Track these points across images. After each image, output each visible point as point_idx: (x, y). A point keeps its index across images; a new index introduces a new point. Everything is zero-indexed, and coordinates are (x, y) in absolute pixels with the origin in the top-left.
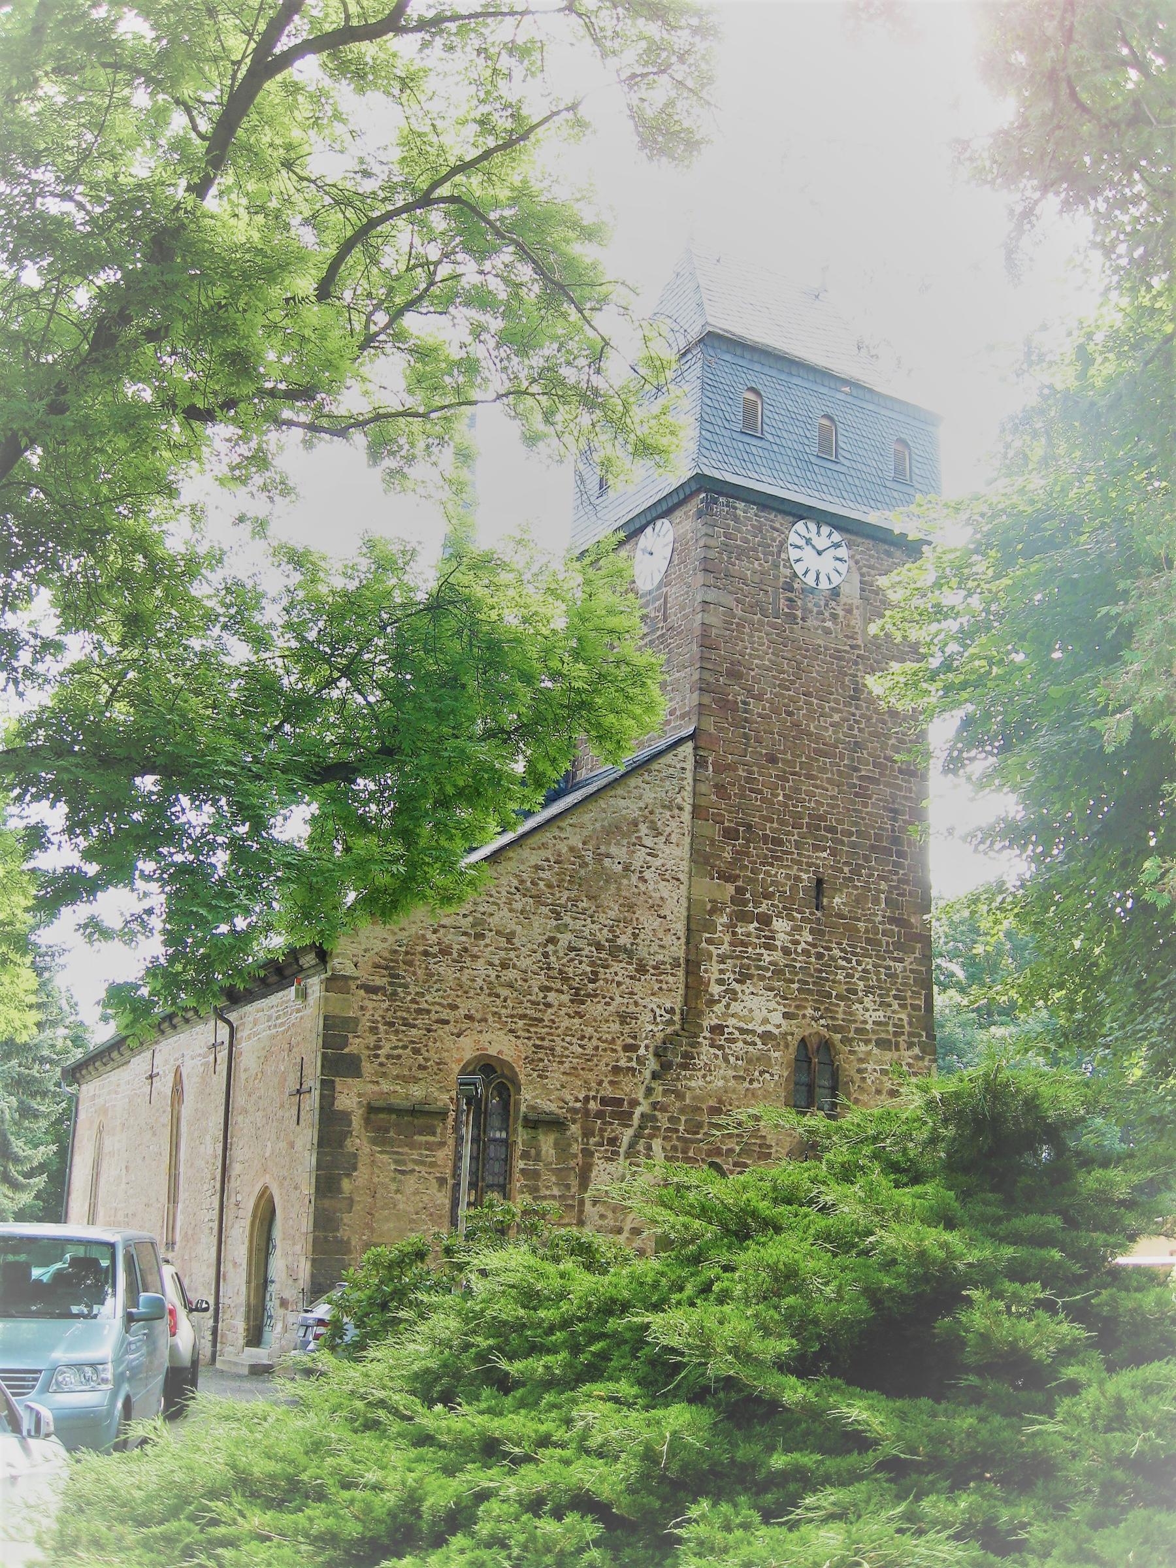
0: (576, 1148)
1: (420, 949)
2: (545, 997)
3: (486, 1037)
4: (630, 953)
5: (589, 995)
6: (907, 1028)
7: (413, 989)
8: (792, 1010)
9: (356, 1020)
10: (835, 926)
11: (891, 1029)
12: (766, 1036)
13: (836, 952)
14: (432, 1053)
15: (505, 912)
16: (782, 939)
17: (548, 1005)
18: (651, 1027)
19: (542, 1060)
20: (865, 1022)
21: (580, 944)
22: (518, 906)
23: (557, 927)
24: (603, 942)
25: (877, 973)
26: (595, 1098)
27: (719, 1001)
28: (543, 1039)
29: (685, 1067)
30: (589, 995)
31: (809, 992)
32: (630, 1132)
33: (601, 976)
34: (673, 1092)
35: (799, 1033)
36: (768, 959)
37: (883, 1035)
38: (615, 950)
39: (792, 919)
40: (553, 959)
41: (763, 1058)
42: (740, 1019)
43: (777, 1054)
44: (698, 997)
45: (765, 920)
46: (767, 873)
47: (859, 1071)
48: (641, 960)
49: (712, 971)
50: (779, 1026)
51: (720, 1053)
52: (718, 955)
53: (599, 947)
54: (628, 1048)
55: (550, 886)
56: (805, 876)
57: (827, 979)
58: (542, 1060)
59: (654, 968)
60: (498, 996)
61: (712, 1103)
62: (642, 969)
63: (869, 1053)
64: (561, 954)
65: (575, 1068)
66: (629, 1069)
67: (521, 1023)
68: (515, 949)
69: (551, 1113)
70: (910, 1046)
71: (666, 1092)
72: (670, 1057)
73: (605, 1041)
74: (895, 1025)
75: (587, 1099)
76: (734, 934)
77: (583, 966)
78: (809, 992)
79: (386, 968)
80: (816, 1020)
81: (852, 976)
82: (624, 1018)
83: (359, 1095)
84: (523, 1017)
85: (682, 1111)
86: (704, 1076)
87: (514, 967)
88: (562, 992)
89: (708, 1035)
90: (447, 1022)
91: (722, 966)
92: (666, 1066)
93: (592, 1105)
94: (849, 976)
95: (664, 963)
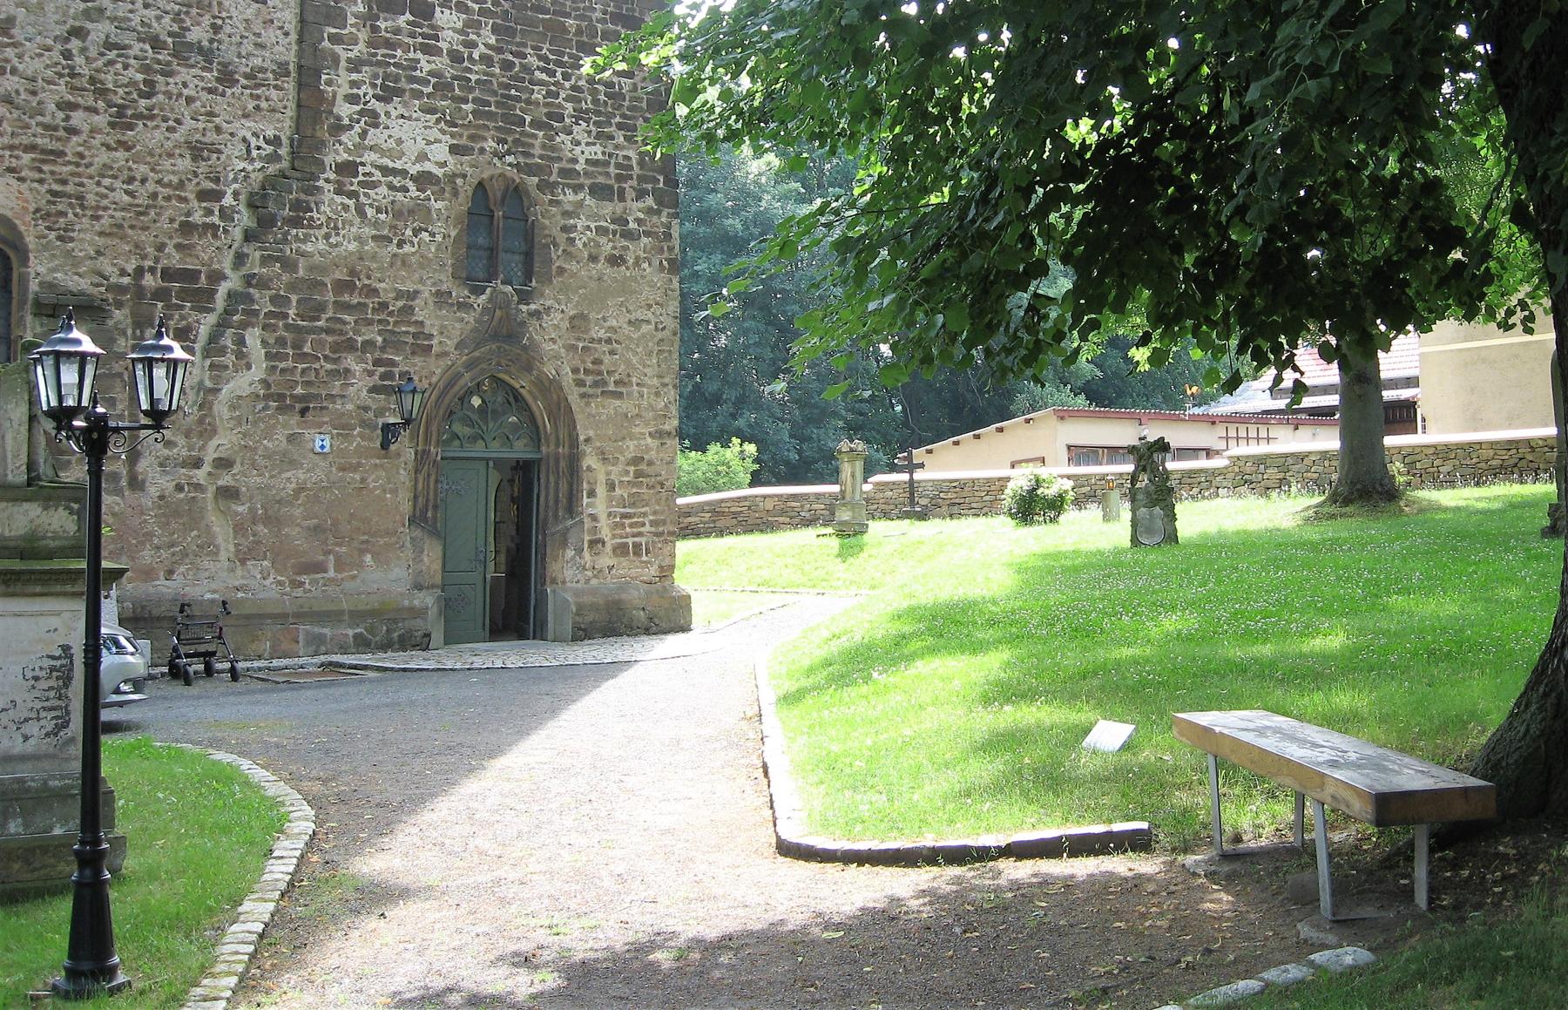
2: (68, 118)
4: (207, 55)
5: (140, 116)
6: (637, 170)
8: (463, 141)
10: (532, 23)
11: (612, 170)
12: (423, 179)
13: (533, 61)
16: (449, 39)
17: (73, 131)
18: (242, 165)
19: (63, 214)
20: (574, 161)
21: (127, 38)
23: (87, 14)
24: (164, 37)
25: (594, 92)
26: (152, 270)
27: (350, 127)
28: (64, 182)
29: (296, 222)
30: (140, 116)
31: (490, 116)
32: (211, 319)
33: (161, 87)
34: (277, 259)
35: (474, 175)
36: (427, 68)
37: (601, 180)
38: (183, 50)
40: (79, 60)
41: (419, 211)
42: (383, 153)
43: (439, 205)
44: (316, 119)
47: (565, 229)
48: (225, 65)
49: (338, 83)
50: (444, 164)
51: (351, 203)
52: (349, 60)
53: (156, 44)
54: (203, 195)
57: (518, 99)
58: (63, 214)
59: (246, 76)
61: (341, 274)
62: (227, 77)
63: (581, 204)
64: (93, 53)
65: (120, 226)
66: (206, 226)
67: (27, 158)
68: (14, 45)
69: (82, 293)
70: (640, 195)
71: (265, 261)
72: (272, 208)
73: (169, 185)
74: (618, 166)
75: (140, 272)
76: (375, 29)
77: (131, 72)
78: (490, 116)
81: (557, 95)
82: (197, 151)
84: (31, 148)
85: (292, 287)
86: (327, 237)
87: (14, 71)
88: (95, 111)
89: (332, 176)
91: (354, 76)
92: (266, 222)
93: (149, 281)
94: (549, 94)
95: (263, 70)
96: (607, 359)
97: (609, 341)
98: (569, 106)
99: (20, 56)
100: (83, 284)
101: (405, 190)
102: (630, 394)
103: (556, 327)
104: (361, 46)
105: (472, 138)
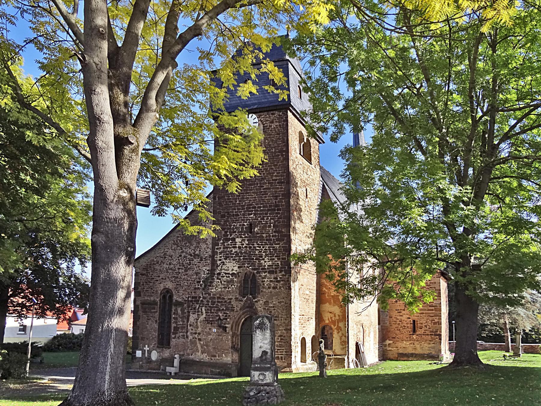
0: (186, 311)
3: (166, 283)
4: (198, 255)
15: (171, 250)
16: (238, 244)
17: (179, 273)
22: (173, 248)
36: (234, 251)
37: (271, 269)
38: (195, 256)
39: (241, 237)
45: (234, 239)
46: (234, 225)
47: (263, 281)
53: (191, 255)
55: (180, 241)
56: (245, 224)
62: (201, 260)
63: (266, 276)
75: (188, 297)
80: (248, 267)
82: (197, 274)
84: (174, 277)
94: (260, 252)
96: (273, 311)
97: (273, 307)
98: (264, 254)
100: (180, 300)
101: (229, 277)
102: (278, 320)
103: (261, 304)
104: (222, 249)
105: (242, 264)
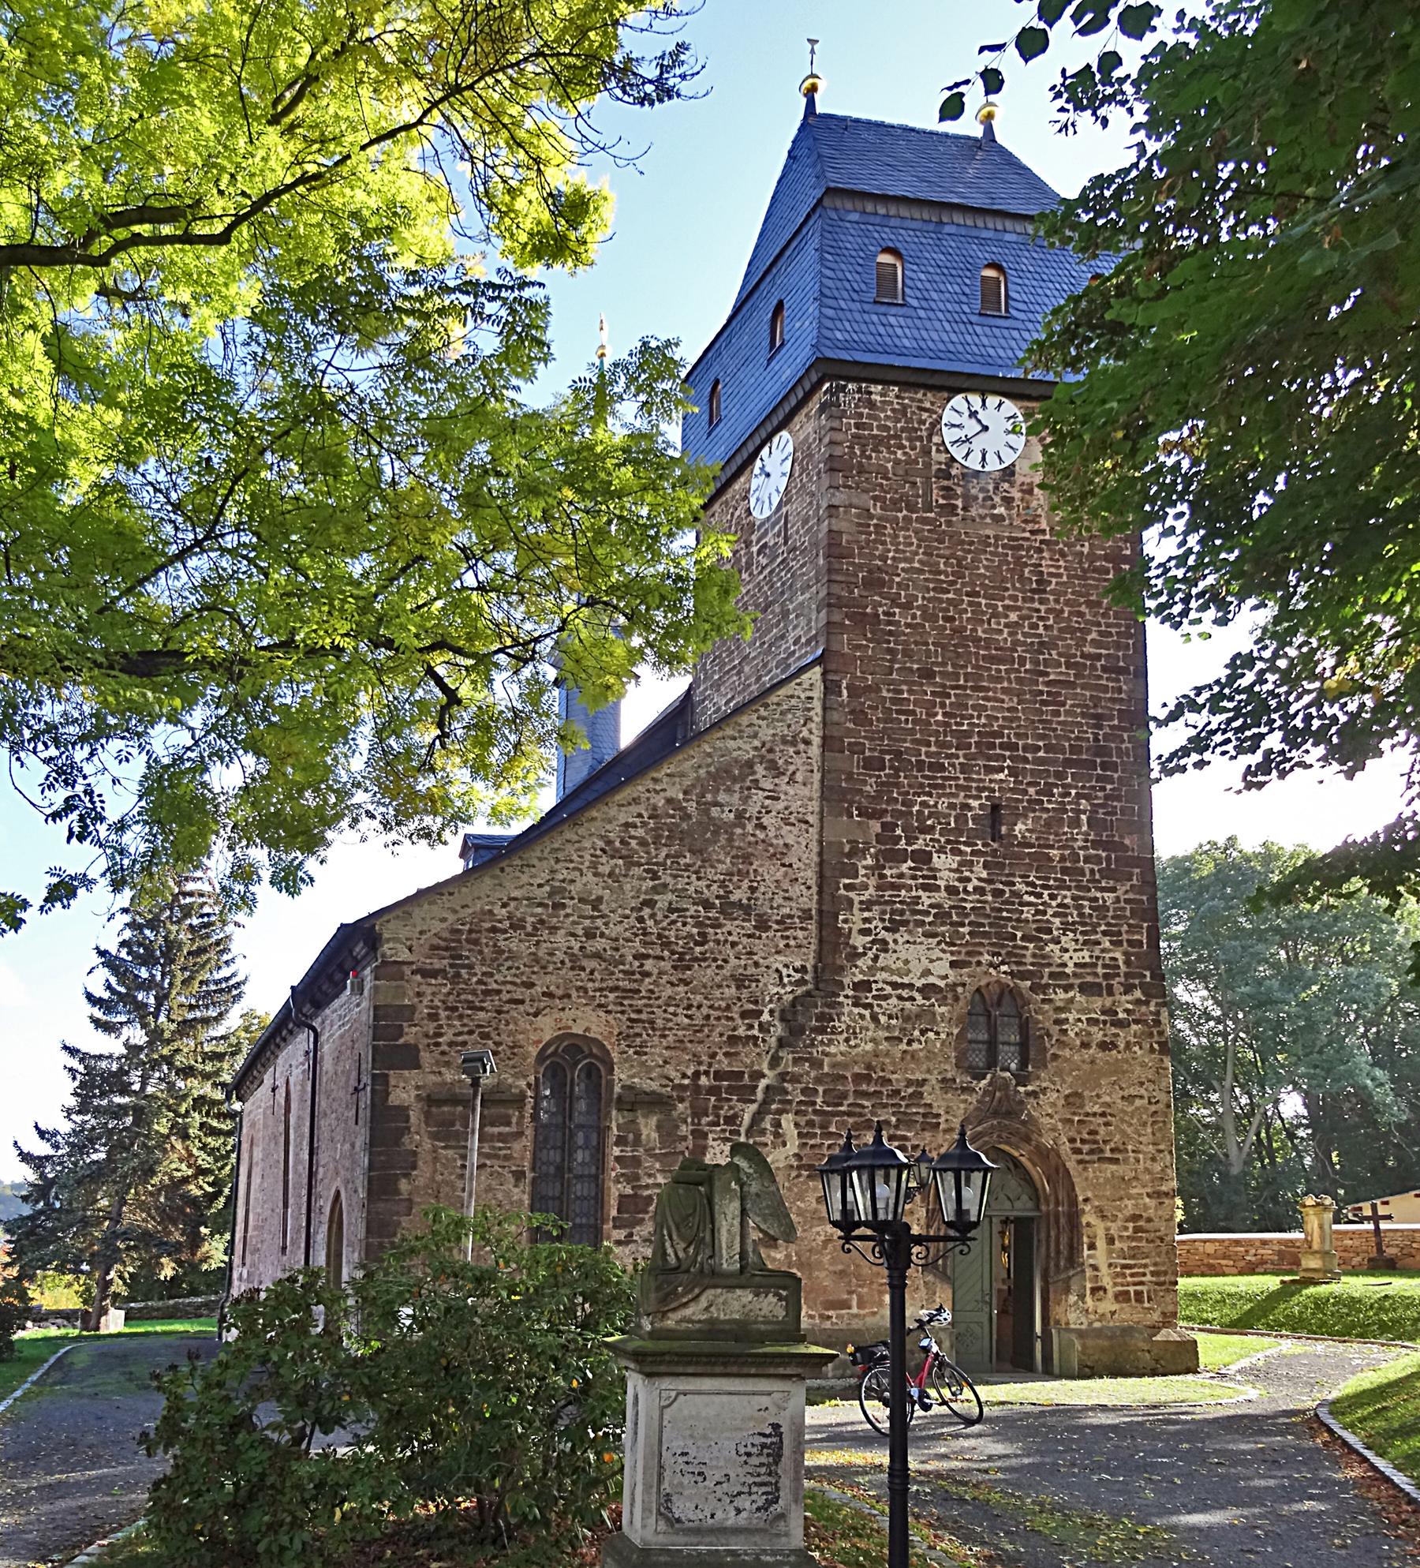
1: (487, 925)
5: (696, 959)
7: (478, 969)
9: (412, 1009)
14: (504, 1037)
15: (589, 877)
22: (606, 869)
53: (707, 905)
55: (643, 843)
60: (583, 969)
75: (697, 1075)
77: (688, 928)
79: (446, 949)
83: (418, 1088)
87: (602, 935)
90: (522, 1002)
99: (606, 924)
